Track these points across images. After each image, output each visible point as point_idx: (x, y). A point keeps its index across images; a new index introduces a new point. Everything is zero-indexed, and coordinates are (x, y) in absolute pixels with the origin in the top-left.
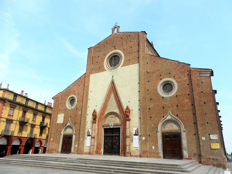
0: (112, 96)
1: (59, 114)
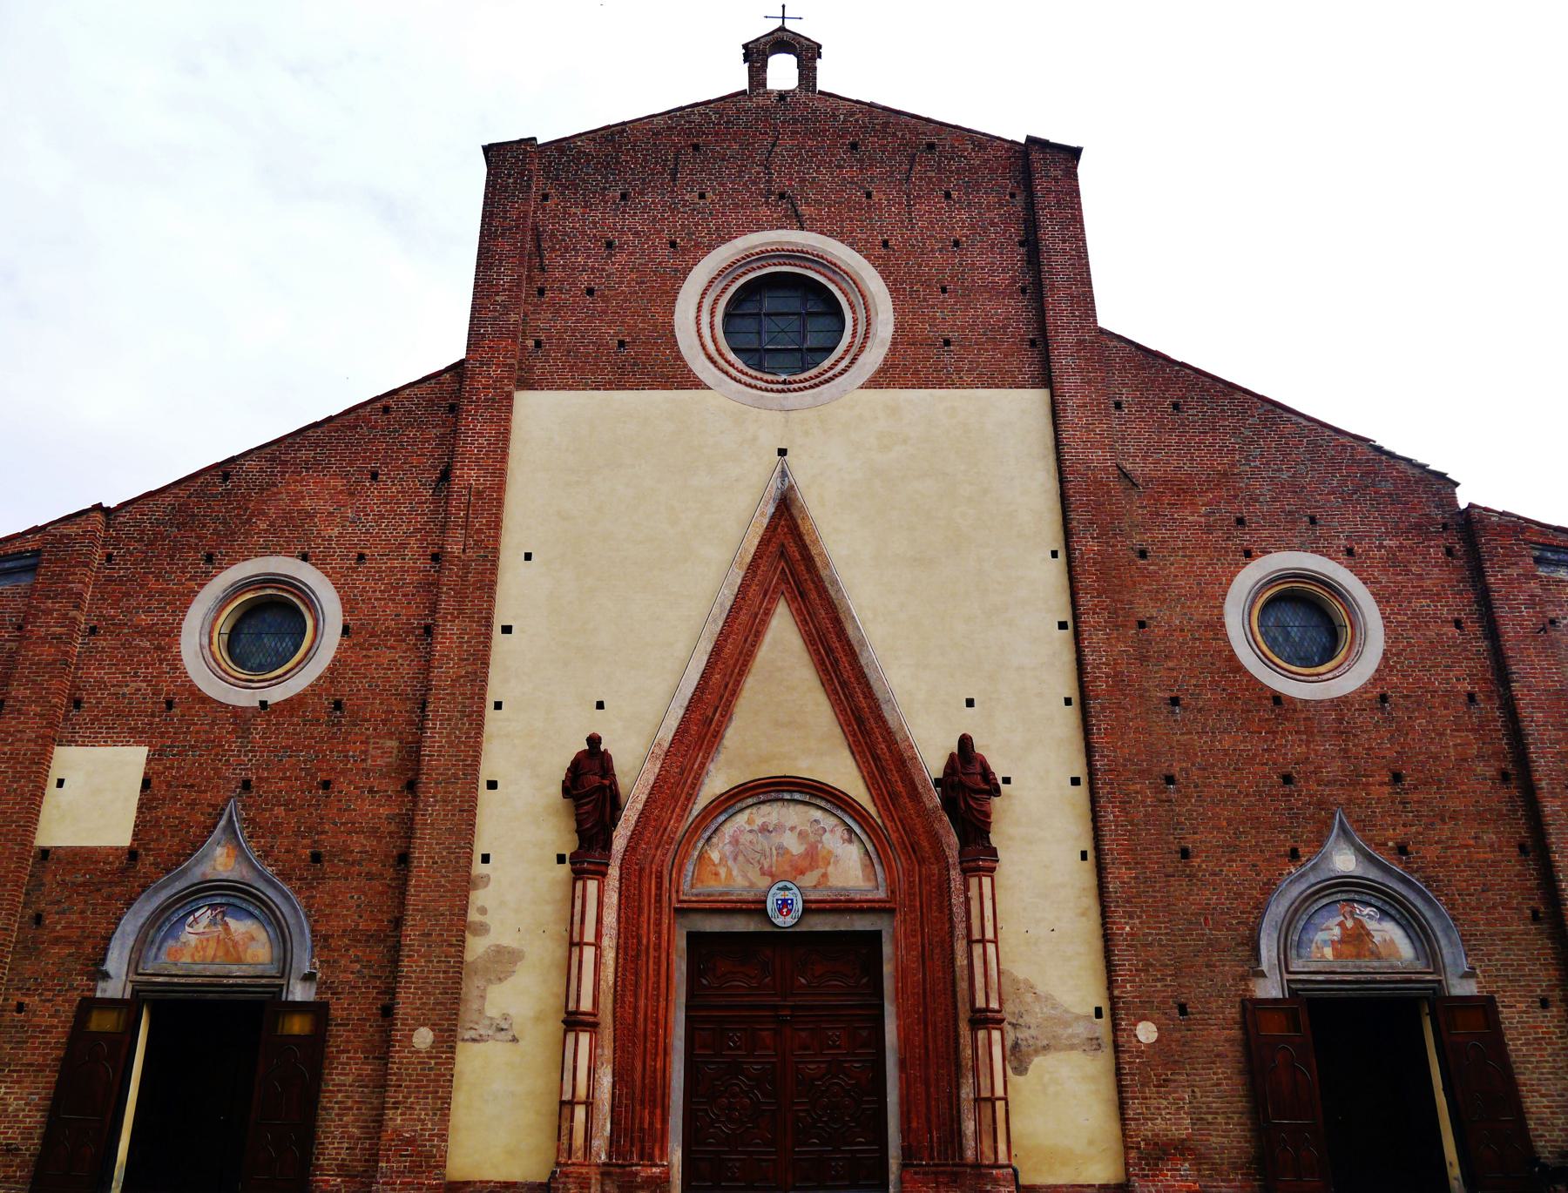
1: (70, 742)
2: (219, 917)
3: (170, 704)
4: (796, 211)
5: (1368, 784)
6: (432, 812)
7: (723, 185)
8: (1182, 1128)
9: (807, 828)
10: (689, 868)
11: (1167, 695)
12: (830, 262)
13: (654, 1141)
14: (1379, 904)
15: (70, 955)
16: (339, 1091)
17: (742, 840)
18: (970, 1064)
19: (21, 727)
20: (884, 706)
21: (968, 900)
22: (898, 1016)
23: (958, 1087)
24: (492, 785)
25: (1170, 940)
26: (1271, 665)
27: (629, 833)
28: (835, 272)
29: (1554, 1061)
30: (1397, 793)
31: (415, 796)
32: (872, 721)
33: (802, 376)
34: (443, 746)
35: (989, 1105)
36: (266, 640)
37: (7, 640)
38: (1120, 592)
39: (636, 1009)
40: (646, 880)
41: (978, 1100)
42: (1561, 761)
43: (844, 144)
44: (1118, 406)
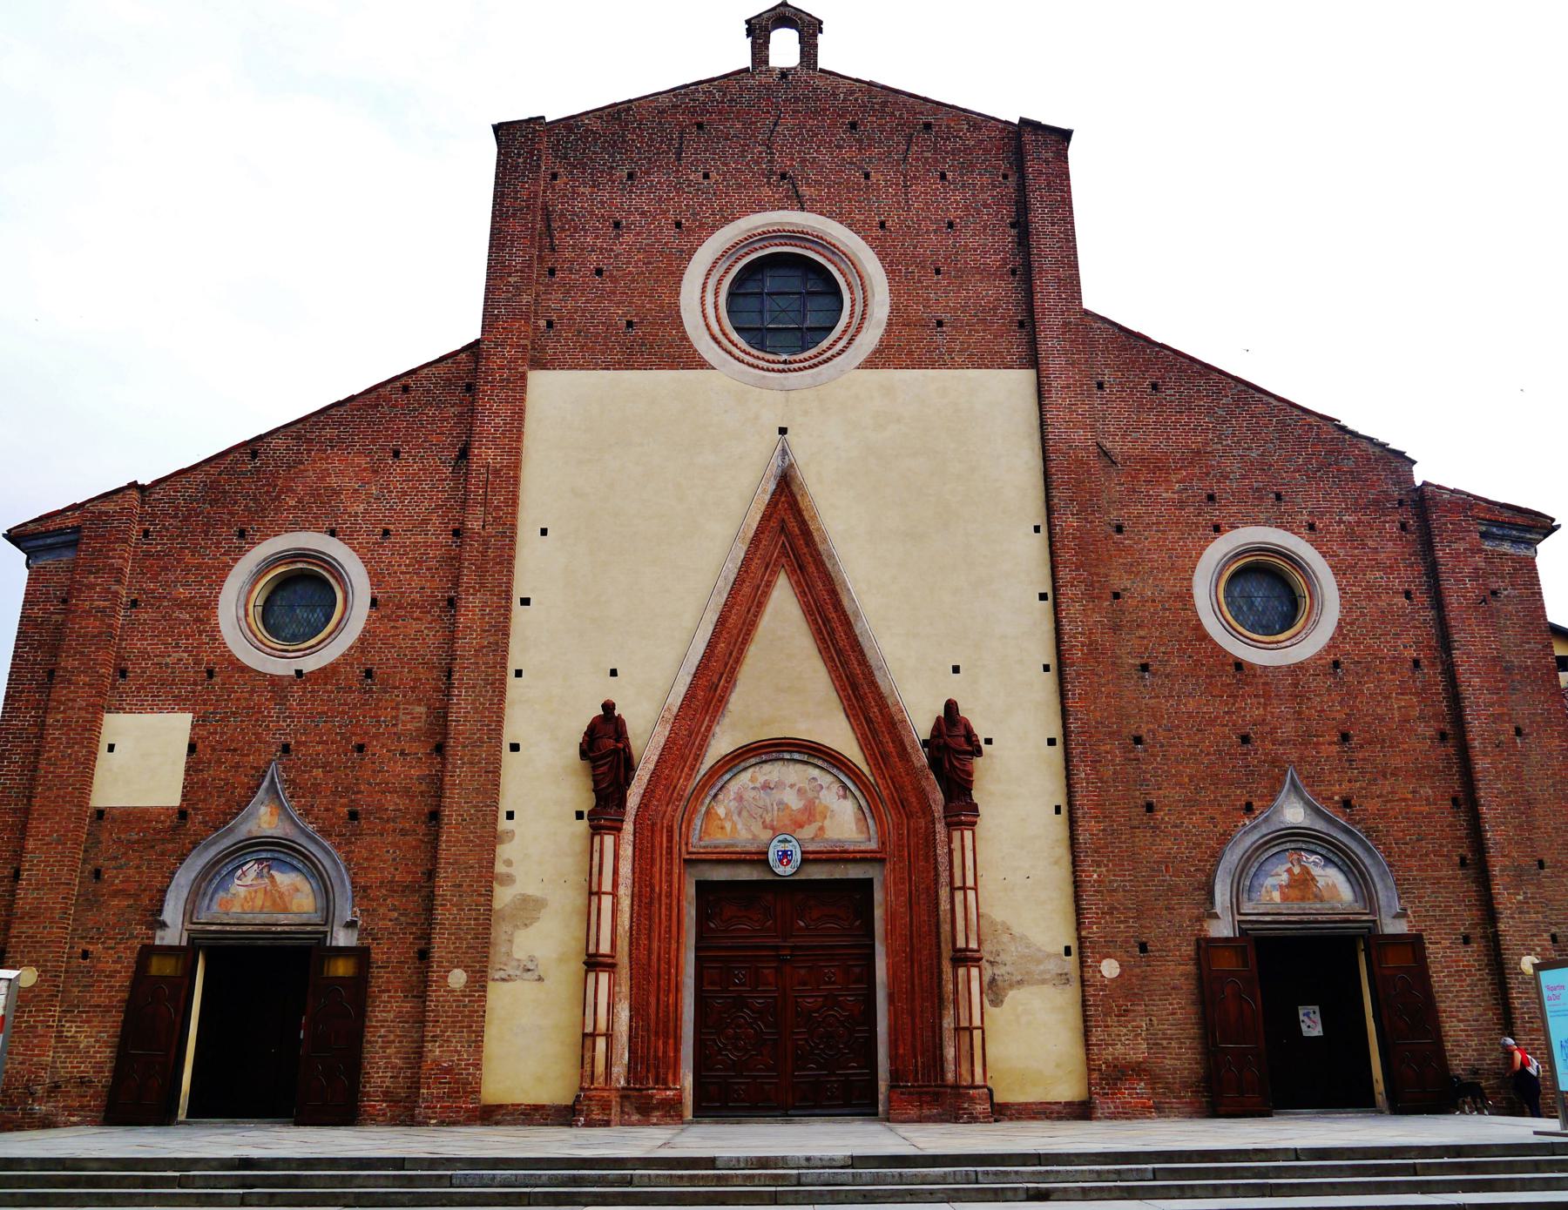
0: (783, 603)
1: (119, 709)
2: (265, 870)
3: (210, 673)
4: (797, 192)
5: (1317, 744)
6: (460, 773)
8: (1139, 1052)
9: (805, 785)
10: (697, 822)
11: (1138, 662)
12: (829, 243)
13: (668, 1068)
14: (1324, 852)
15: (129, 906)
16: (382, 1026)
17: (746, 796)
18: (951, 997)
19: (72, 696)
20: (876, 673)
21: (951, 852)
22: (887, 955)
23: (941, 1018)
24: (515, 747)
25: (1131, 886)
26: (1234, 633)
27: (642, 791)
28: (834, 253)
29: (1472, 991)
30: (1345, 752)
31: (444, 758)
32: (865, 686)
33: (801, 356)
34: (469, 712)
35: (968, 1033)
36: (298, 611)
37: (52, 613)
38: (1096, 566)
39: (650, 950)
40: (657, 834)
41: (958, 1029)
42: (1494, 722)
43: (843, 123)
44: (1100, 386)
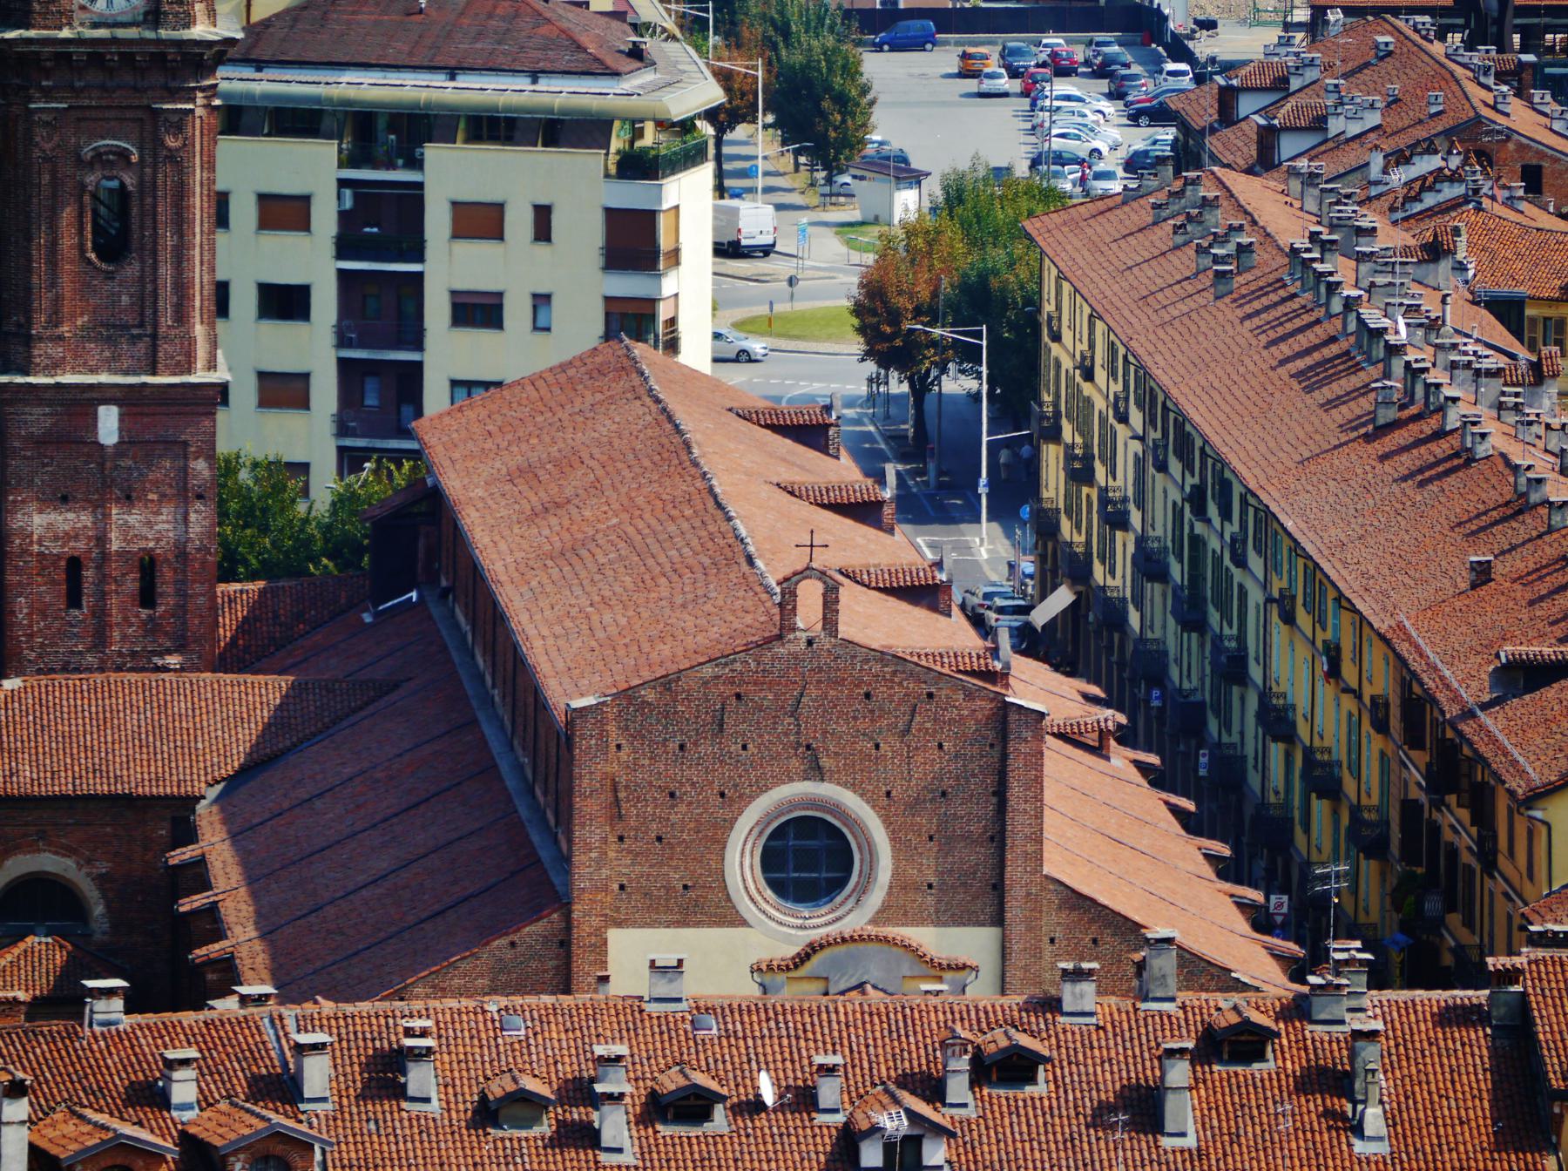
7: (761, 736)
